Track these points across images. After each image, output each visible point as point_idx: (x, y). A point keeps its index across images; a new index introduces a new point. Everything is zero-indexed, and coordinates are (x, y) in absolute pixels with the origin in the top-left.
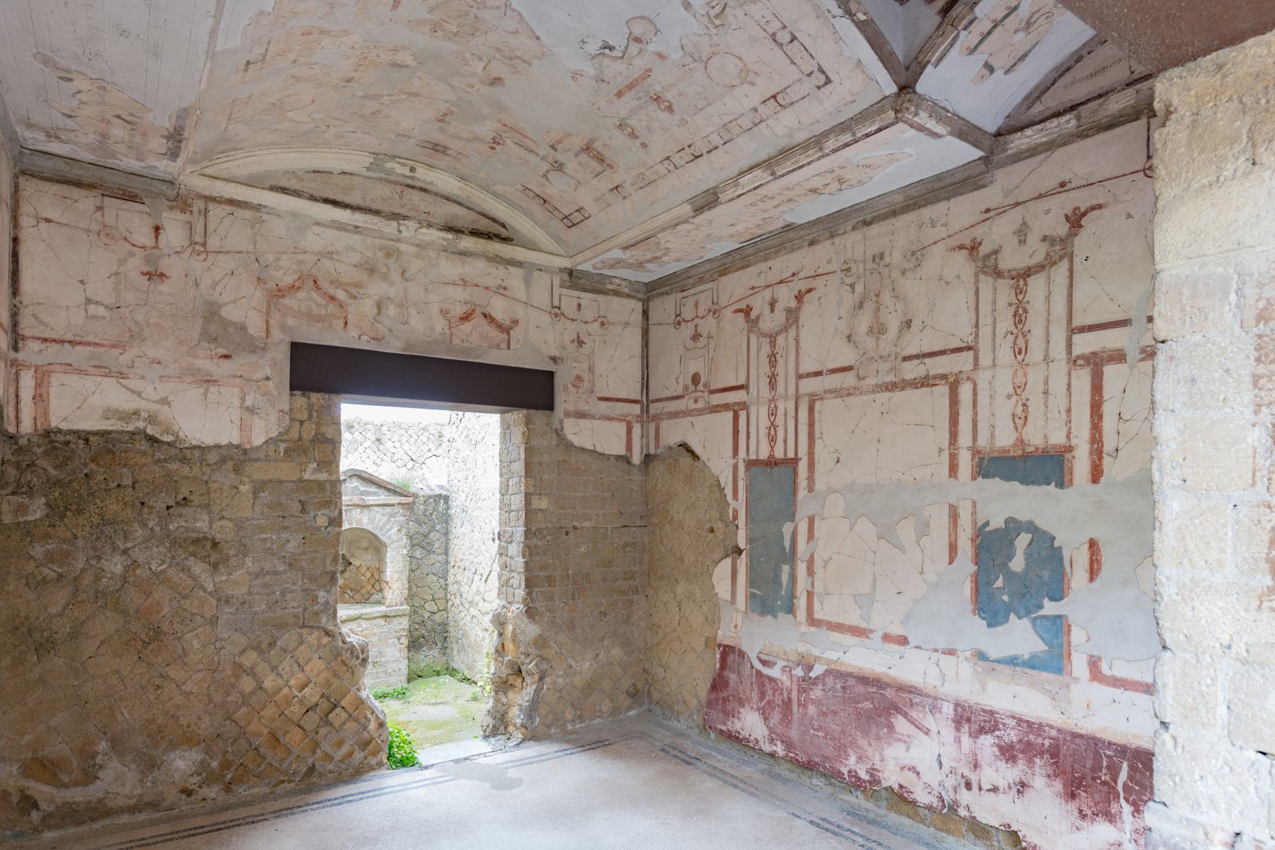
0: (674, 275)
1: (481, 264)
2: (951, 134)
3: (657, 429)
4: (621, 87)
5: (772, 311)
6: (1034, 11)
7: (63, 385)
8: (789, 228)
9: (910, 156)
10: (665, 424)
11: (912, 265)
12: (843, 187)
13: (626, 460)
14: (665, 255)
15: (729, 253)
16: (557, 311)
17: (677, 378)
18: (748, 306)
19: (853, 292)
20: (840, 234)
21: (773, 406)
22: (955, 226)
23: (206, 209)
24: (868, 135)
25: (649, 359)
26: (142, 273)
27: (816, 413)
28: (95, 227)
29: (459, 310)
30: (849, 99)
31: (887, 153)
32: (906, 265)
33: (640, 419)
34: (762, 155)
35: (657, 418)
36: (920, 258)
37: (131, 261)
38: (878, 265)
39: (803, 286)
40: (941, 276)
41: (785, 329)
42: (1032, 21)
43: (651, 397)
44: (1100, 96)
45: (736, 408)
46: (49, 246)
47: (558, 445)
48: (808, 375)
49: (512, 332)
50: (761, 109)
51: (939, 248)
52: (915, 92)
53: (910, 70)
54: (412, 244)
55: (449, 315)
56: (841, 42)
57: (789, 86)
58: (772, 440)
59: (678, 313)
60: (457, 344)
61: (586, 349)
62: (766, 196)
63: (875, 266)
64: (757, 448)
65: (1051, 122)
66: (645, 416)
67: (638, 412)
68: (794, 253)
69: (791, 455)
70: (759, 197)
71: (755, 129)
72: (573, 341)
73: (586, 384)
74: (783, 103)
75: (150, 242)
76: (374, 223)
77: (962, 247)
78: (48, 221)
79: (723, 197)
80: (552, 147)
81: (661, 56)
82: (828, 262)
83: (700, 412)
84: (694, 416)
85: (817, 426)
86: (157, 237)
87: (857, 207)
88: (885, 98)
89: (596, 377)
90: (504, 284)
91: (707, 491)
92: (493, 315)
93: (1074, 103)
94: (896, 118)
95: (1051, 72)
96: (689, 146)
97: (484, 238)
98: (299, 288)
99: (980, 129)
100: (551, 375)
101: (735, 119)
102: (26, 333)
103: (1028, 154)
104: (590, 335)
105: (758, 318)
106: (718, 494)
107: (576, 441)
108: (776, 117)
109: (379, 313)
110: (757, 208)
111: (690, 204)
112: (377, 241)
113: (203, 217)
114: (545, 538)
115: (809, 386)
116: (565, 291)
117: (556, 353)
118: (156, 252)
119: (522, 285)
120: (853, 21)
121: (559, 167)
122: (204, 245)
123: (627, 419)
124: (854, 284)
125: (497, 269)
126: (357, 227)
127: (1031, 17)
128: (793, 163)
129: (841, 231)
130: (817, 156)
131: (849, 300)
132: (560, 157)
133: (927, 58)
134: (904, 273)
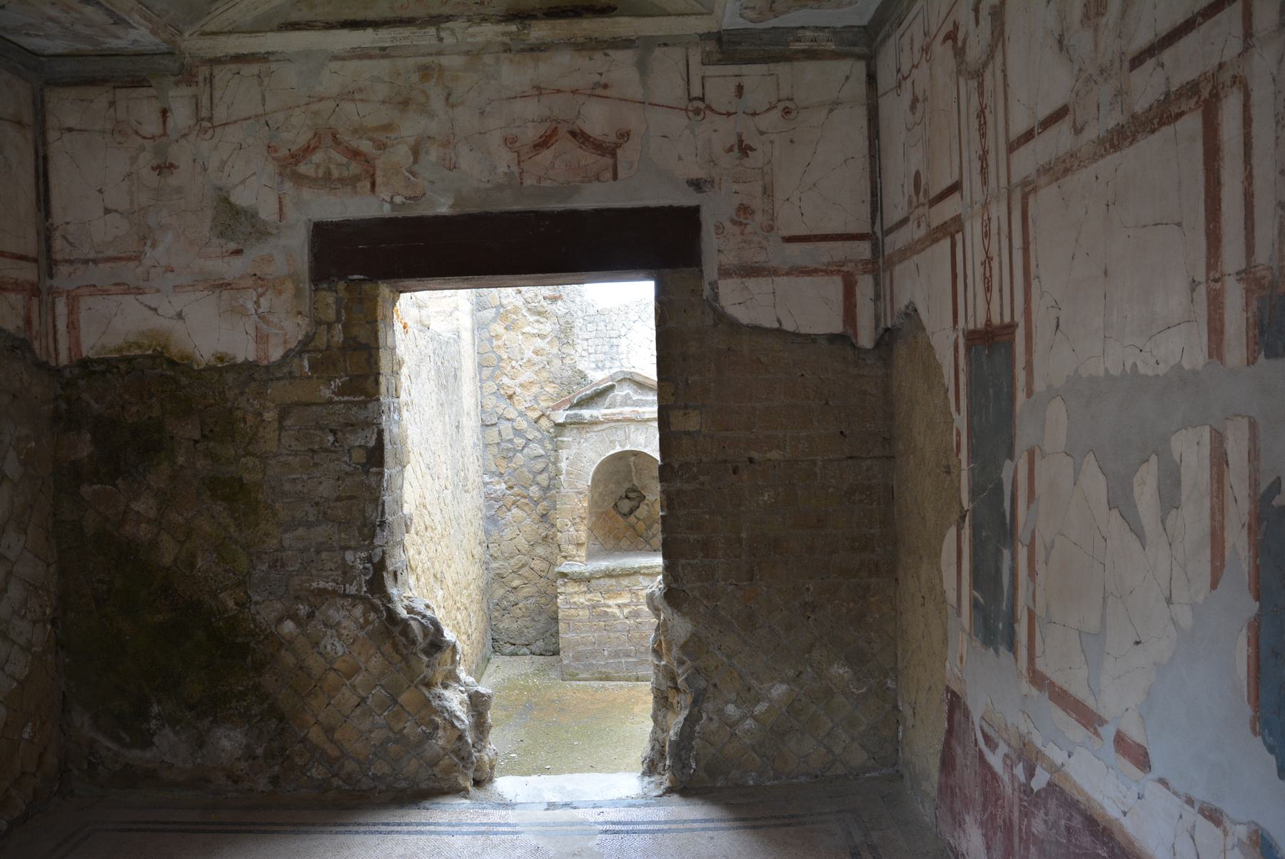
1: (564, 58)
7: (90, 309)
13: (843, 340)
16: (700, 104)
23: (211, 75)
26: (152, 168)
27: (1030, 220)
29: (532, 134)
35: (890, 264)
43: (885, 227)
45: (952, 229)
46: (72, 157)
47: (715, 325)
49: (619, 152)
54: (459, 54)
55: (517, 145)
60: (532, 185)
61: (756, 160)
69: (1007, 319)
72: (731, 149)
73: (759, 217)
76: (405, 38)
85: (1032, 247)
86: (164, 122)
90: (603, 80)
92: (587, 129)
97: (568, 17)
98: (315, 148)
100: (695, 210)
102: (58, 257)
104: (762, 133)
107: (743, 315)
109: (416, 161)
112: (411, 62)
113: (208, 85)
116: (711, 70)
117: (697, 173)
119: (634, 75)
122: (210, 119)
123: (845, 269)
125: (591, 59)
126: (383, 49)
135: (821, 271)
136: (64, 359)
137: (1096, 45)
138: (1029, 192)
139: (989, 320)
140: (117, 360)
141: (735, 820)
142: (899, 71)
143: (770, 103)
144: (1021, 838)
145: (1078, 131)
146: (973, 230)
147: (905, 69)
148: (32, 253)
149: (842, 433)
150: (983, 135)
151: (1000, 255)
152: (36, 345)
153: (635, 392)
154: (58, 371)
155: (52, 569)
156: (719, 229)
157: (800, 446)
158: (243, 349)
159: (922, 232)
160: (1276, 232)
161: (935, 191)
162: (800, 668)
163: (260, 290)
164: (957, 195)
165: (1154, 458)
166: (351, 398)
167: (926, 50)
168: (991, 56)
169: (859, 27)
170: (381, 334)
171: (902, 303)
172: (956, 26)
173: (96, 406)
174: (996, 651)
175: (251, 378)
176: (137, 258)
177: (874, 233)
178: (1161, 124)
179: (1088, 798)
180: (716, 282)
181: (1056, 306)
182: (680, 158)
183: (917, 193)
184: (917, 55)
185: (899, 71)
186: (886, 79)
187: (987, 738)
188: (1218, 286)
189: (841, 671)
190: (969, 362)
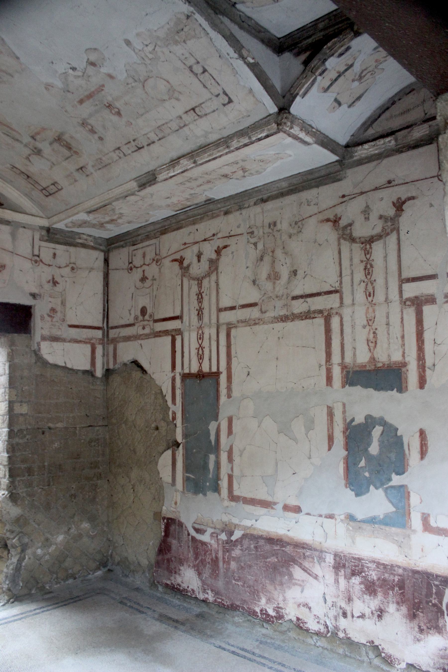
0: (128, 233)
2: (316, 143)
3: (115, 350)
4: (82, 97)
5: (199, 261)
6: (363, 69)
8: (209, 201)
9: (290, 156)
10: (121, 346)
11: (295, 231)
12: (246, 174)
13: (90, 373)
14: (119, 218)
15: (167, 218)
16: (37, 258)
17: (130, 311)
18: (181, 257)
19: (256, 248)
20: (245, 208)
21: (200, 332)
22: (324, 206)
24: (260, 140)
25: (110, 295)
27: (232, 337)
30: (245, 114)
31: (274, 153)
32: (292, 231)
33: (102, 342)
34: (187, 148)
35: (115, 341)
36: (301, 226)
38: (273, 230)
39: (221, 243)
40: (316, 240)
41: (208, 275)
42: (363, 75)
43: (110, 325)
44: (408, 127)
45: (173, 333)
47: (36, 363)
48: (226, 309)
50: (184, 117)
51: (313, 221)
52: (289, 113)
53: (286, 98)
56: (237, 75)
57: (203, 103)
58: (201, 358)
59: (130, 261)
61: (59, 288)
62: (191, 178)
63: (270, 231)
64: (190, 364)
65: (380, 141)
66: (106, 339)
68: (214, 219)
69: (214, 369)
70: (186, 179)
71: (180, 131)
72: (49, 282)
73: (59, 314)
74: (199, 114)
77: (328, 220)
79: (161, 177)
80: (33, 137)
81: (111, 77)
82: (238, 227)
83: (147, 336)
84: (142, 339)
85: (233, 347)
87: (257, 189)
88: (270, 115)
89: (67, 310)
91: (153, 397)
93: (393, 130)
94: (278, 129)
95: (377, 109)
96: (134, 140)
99: (335, 142)
101: (167, 123)
103: (366, 161)
104: (62, 277)
105: (189, 266)
106: (161, 401)
107: (51, 359)
108: (195, 123)
110: (185, 186)
111: (136, 181)
114: (25, 437)
116: (43, 244)
119: (9, 238)
120: (245, 62)
121: (38, 152)
123: (92, 341)
124: (257, 243)
127: (362, 73)
128: (210, 155)
129: (246, 205)
130: (225, 152)
131: (254, 254)
132: (40, 145)
133: (296, 92)
134: (290, 237)
135: (83, 341)
137: (274, 288)
141: (54, 604)
143: (66, 263)
144: (224, 562)
149: (86, 415)
156: (42, 318)
157: (70, 421)
160: (352, 355)
162: (70, 527)
169: (105, 239)
174: (205, 495)
177: (103, 327)
178: (306, 318)
179: (268, 532)
180: (40, 343)
182: (27, 282)
187: (198, 531)
188: (331, 366)
189: (86, 525)
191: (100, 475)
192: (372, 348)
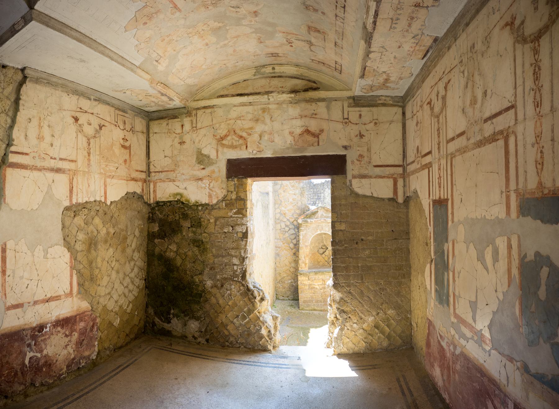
13: (393, 200)
15: (422, 68)
26: (179, 143)
28: (166, 131)
35: (409, 175)
37: (176, 139)
47: (351, 194)
67: (401, 172)
69: (446, 197)
75: (181, 132)
78: (156, 133)
107: (360, 191)
115: (452, 147)
118: (182, 134)
123: (394, 176)
136: (152, 201)
138: (453, 157)
139: (440, 197)
140: (167, 202)
142: (412, 112)
144: (453, 371)
145: (468, 139)
146: (435, 167)
147: (415, 112)
148: (145, 170)
150: (439, 137)
151: (443, 176)
152: (145, 197)
153: (325, 213)
154: (149, 205)
155: (146, 264)
158: (204, 200)
159: (419, 166)
161: (423, 153)
163: (210, 181)
164: (430, 155)
165: (491, 246)
166: (238, 216)
167: (421, 106)
168: (442, 112)
170: (248, 196)
171: (412, 188)
172: (431, 100)
173: (160, 215)
174: (443, 306)
175: (207, 208)
176: (174, 171)
181: (461, 194)
183: (418, 153)
184: (418, 108)
185: (412, 112)
186: (408, 114)
190: (434, 210)
191: (404, 275)
192: (539, 171)
